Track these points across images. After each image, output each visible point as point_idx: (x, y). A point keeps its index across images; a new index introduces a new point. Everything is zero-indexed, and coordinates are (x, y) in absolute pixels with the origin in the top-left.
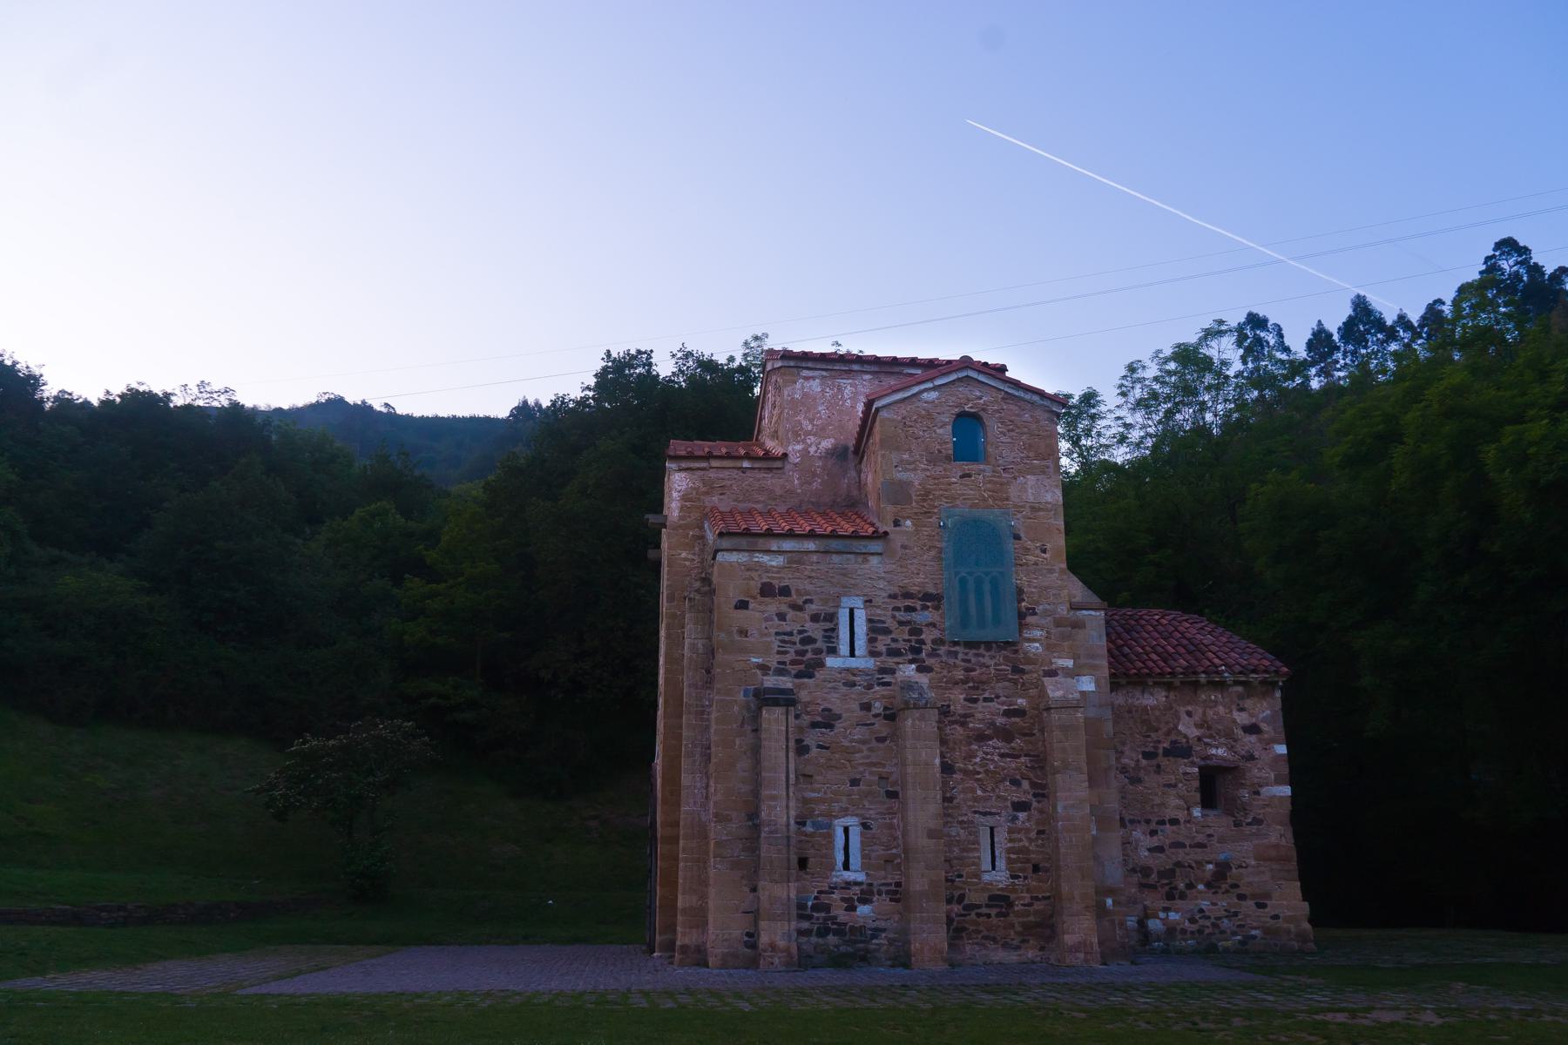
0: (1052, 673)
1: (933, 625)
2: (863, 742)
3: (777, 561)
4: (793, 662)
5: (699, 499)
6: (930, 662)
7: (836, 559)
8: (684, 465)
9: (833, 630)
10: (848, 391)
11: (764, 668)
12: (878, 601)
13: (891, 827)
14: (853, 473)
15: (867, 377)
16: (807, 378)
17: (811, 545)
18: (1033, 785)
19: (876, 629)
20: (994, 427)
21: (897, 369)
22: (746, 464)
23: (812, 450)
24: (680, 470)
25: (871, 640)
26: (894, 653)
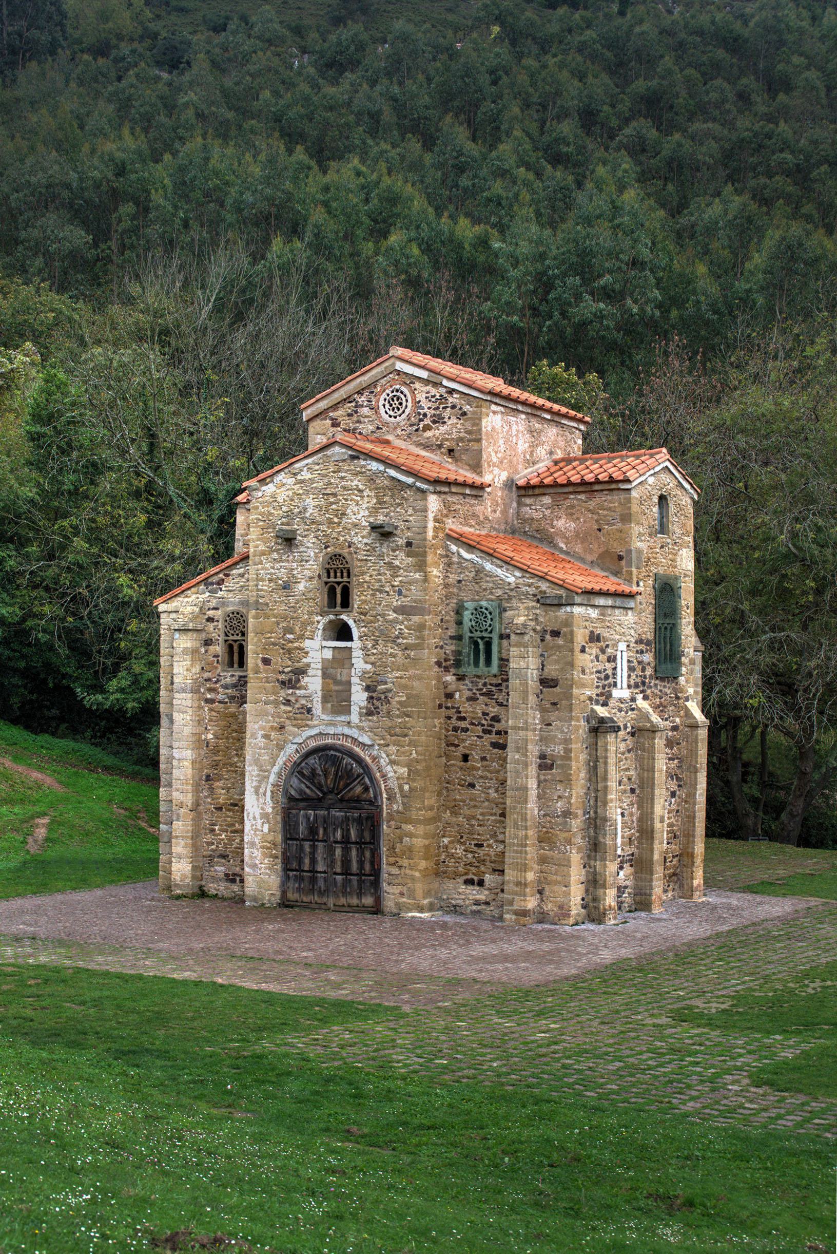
0: (687, 699)
1: (649, 664)
2: (623, 754)
3: (594, 613)
4: (602, 694)
5: (444, 523)
6: (649, 692)
7: (617, 611)
8: (438, 489)
9: (615, 669)
10: (514, 427)
11: (590, 699)
12: (632, 645)
13: (631, 814)
14: (515, 505)
15: (523, 416)
16: (494, 412)
17: (610, 602)
18: (678, 779)
19: (631, 669)
20: (672, 509)
21: (539, 413)
22: (468, 491)
23: (496, 480)
24: (435, 493)
25: (629, 676)
26: (636, 686)
